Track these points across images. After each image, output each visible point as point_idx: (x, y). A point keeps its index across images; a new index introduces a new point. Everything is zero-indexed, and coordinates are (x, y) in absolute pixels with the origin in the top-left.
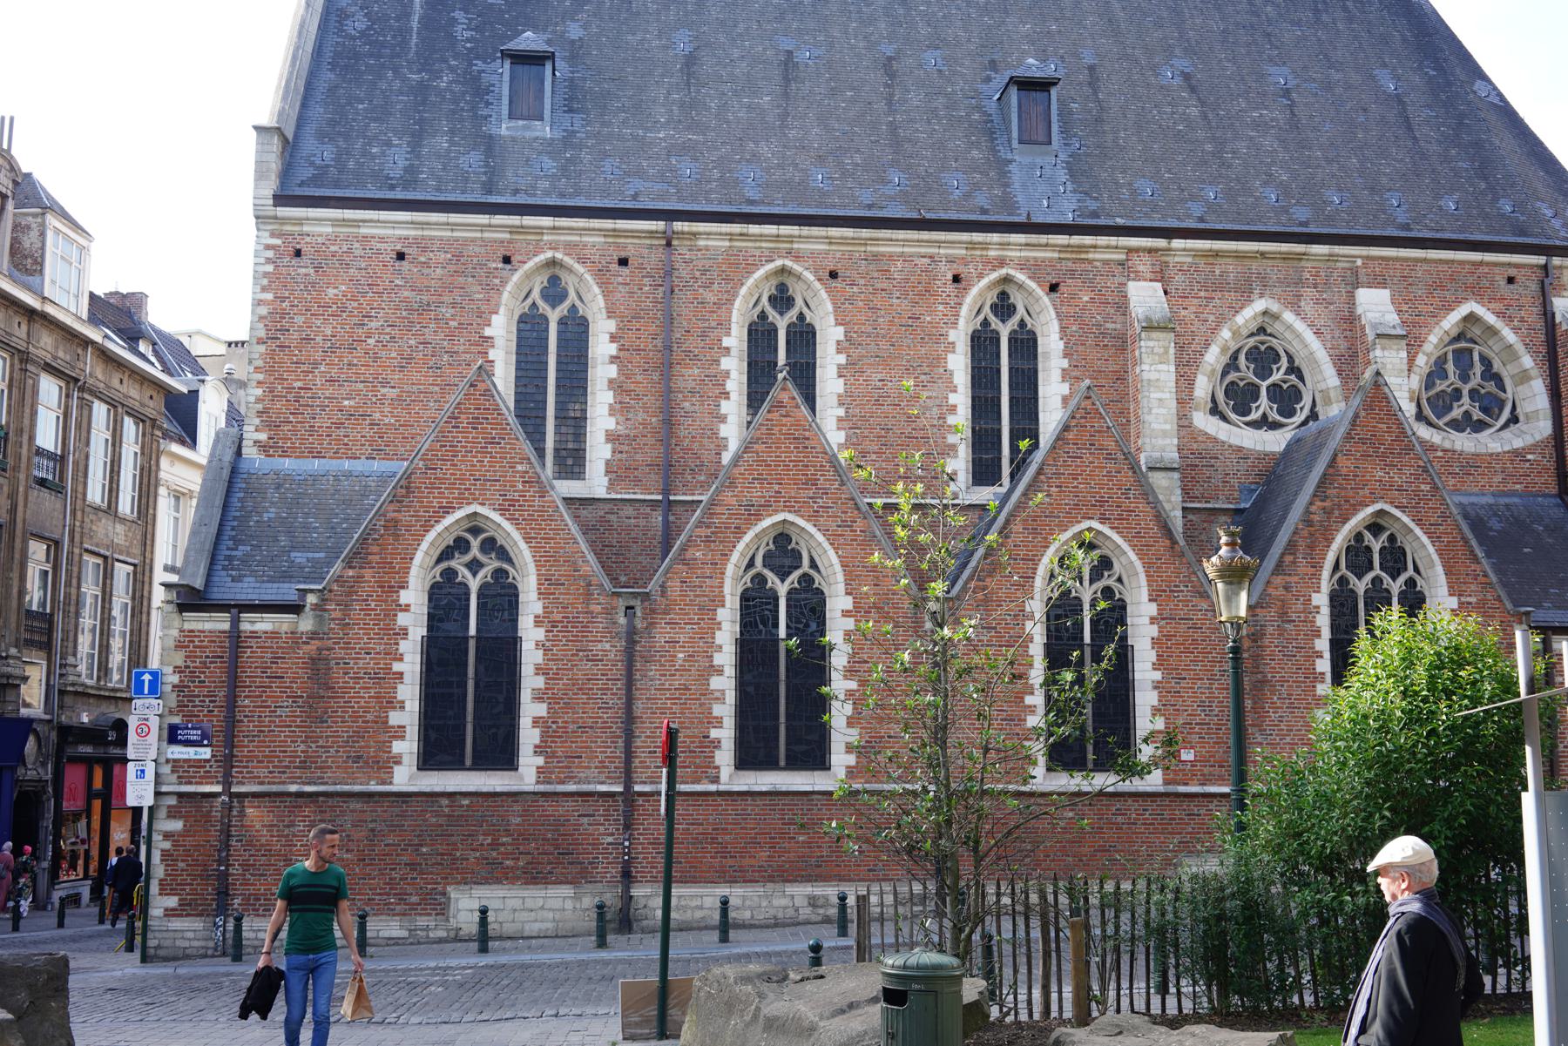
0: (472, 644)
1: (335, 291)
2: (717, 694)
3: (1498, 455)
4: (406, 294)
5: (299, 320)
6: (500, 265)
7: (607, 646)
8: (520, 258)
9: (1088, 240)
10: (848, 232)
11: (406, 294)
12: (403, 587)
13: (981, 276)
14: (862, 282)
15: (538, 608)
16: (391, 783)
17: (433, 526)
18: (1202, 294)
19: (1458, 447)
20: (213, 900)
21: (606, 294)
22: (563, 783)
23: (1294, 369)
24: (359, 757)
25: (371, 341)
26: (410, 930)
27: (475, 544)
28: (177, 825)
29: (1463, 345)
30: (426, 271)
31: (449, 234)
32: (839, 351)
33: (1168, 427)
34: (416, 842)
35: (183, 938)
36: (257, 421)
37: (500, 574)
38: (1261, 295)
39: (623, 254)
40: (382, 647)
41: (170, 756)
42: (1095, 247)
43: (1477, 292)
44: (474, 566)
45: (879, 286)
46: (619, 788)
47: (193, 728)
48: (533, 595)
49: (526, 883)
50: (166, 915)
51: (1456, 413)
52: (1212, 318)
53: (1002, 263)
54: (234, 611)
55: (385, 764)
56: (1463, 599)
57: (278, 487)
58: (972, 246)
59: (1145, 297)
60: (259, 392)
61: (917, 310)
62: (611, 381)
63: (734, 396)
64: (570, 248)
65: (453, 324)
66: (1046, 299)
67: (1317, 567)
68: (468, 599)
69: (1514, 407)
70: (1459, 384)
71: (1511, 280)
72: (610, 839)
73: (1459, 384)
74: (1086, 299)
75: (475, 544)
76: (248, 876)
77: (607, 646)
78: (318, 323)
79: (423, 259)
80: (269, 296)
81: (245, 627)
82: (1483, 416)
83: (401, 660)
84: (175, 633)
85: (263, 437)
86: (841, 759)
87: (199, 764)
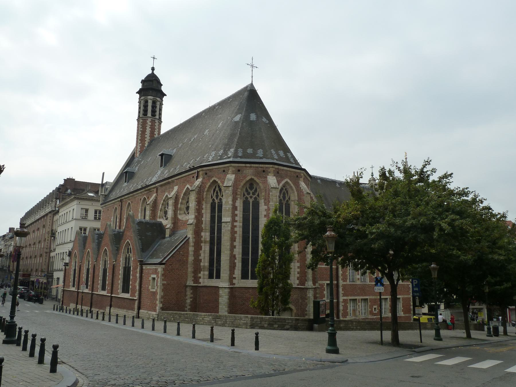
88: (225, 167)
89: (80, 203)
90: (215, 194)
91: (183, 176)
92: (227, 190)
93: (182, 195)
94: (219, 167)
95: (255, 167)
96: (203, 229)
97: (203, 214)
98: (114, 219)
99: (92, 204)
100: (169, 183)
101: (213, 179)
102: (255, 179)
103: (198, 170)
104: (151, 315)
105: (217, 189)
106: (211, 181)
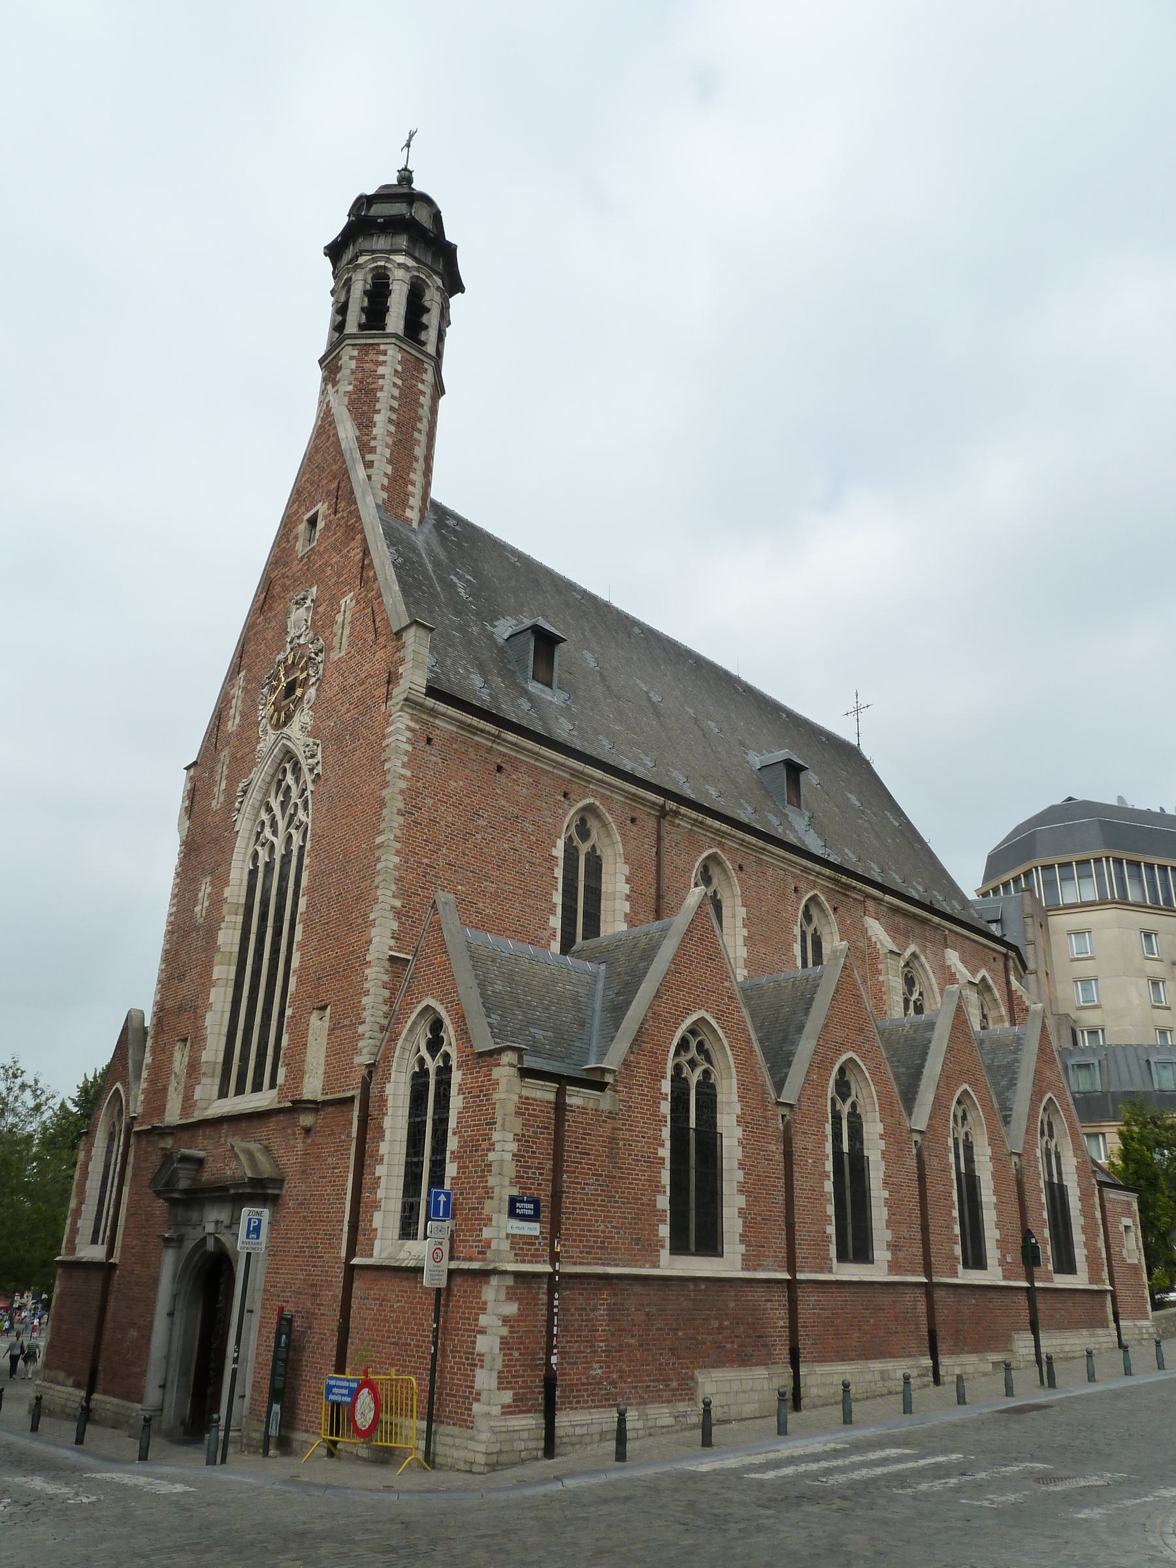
0: (692, 1134)
1: (455, 784)
4: (503, 803)
5: (429, 801)
6: (563, 799)
7: (774, 1148)
8: (575, 797)
9: (854, 883)
11: (503, 803)
12: (663, 1077)
13: (807, 892)
15: (737, 1109)
16: (658, 1267)
17: (680, 1024)
20: (539, 1393)
21: (625, 844)
22: (755, 1270)
24: (639, 1239)
26: (676, 1417)
27: (693, 1044)
28: (512, 1309)
30: (516, 787)
31: (532, 762)
32: (744, 926)
34: (674, 1326)
35: (520, 1439)
36: (394, 887)
37: (706, 1073)
39: (634, 815)
40: (652, 1132)
41: (510, 1231)
42: (854, 888)
43: (985, 964)
44: (693, 1064)
45: (761, 883)
46: (786, 1276)
47: (528, 1202)
48: (735, 1098)
49: (740, 1366)
50: (503, 1413)
53: (814, 885)
54: (563, 1082)
55: (650, 1251)
57: (494, 961)
58: (806, 870)
59: (876, 929)
60: (397, 860)
62: (626, 915)
64: (604, 798)
68: (688, 1095)
72: (781, 1323)
75: (693, 1044)
76: (565, 1365)
77: (774, 1148)
78: (443, 808)
79: (515, 777)
80: (408, 773)
81: (568, 1100)
83: (663, 1146)
84: (516, 1098)
85: (398, 903)
86: (881, 1254)
87: (529, 1240)
100: (924, 922)
104: (1144, 1331)
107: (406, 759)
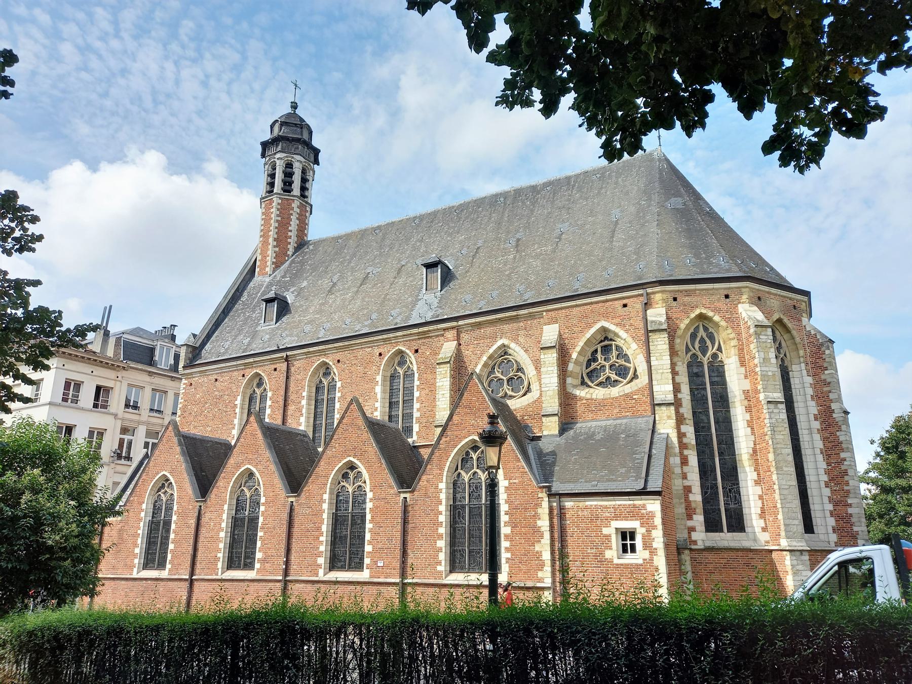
2: (221, 539)
3: (616, 398)
10: (341, 344)
11: (216, 393)
14: (348, 362)
18: (475, 342)
19: (594, 397)
23: (520, 369)
25: (206, 411)
29: (606, 343)
33: (446, 406)
38: (501, 338)
43: (606, 316)
45: (353, 363)
51: (602, 378)
52: (479, 352)
56: (511, 481)
61: (366, 370)
63: (304, 415)
65: (227, 401)
66: (412, 357)
67: (442, 469)
69: (636, 370)
70: (603, 363)
71: (625, 306)
73: (603, 363)
74: (428, 353)
82: (617, 378)
88: (729, 288)
89: (64, 365)
90: (697, 345)
91: (580, 303)
92: (763, 333)
93: (581, 344)
94: (715, 287)
95: (782, 296)
96: (685, 419)
97: (679, 384)
98: (243, 400)
99: (92, 372)
101: (697, 312)
102: (786, 320)
103: (649, 290)
105: (702, 333)
106: (693, 315)
107: (182, 396)
